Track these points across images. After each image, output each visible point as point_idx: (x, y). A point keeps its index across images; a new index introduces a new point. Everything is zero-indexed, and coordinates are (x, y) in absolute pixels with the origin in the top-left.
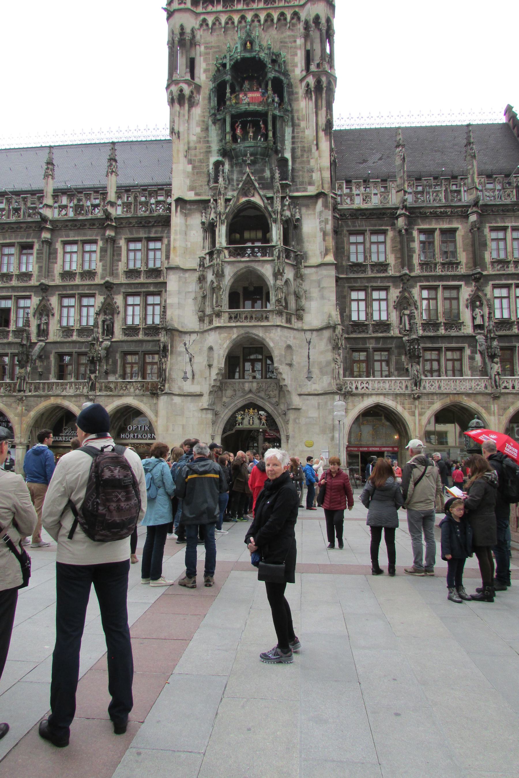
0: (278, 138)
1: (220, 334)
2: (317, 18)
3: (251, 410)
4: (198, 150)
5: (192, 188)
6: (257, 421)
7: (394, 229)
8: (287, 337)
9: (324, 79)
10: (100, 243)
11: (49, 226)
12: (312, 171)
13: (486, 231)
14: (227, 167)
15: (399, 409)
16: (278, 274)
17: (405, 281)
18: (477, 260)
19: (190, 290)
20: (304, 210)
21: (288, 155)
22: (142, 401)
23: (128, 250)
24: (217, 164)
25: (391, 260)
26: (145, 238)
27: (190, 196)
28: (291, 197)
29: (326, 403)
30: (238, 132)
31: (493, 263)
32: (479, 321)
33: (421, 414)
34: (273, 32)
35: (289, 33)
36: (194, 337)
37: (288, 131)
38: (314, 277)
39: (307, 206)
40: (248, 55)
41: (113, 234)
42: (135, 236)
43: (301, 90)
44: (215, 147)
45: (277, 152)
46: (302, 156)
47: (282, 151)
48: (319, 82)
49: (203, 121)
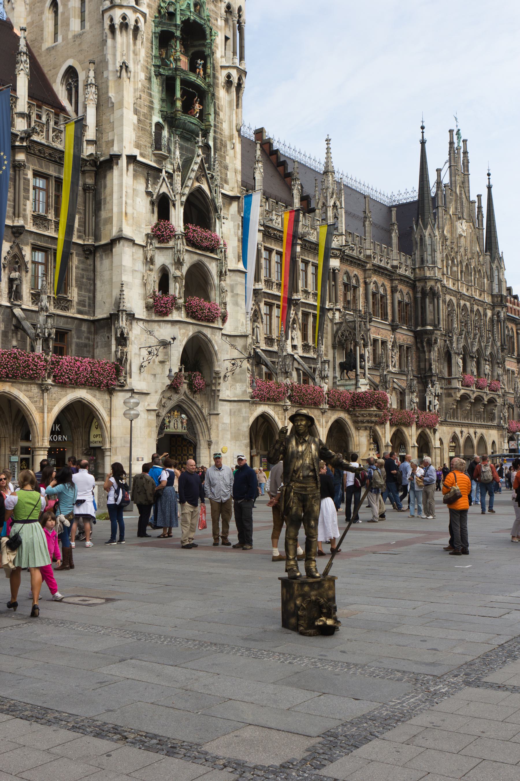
1: (180, 329)
3: (176, 413)
4: (142, 101)
5: (138, 146)
6: (180, 425)
14: (165, 133)
19: (136, 269)
21: (211, 143)
22: (95, 396)
26: (55, 177)
29: (240, 411)
32: (295, 343)
36: (141, 323)
40: (198, 20)
42: (44, 170)
44: (157, 105)
46: (221, 148)
49: (147, 68)
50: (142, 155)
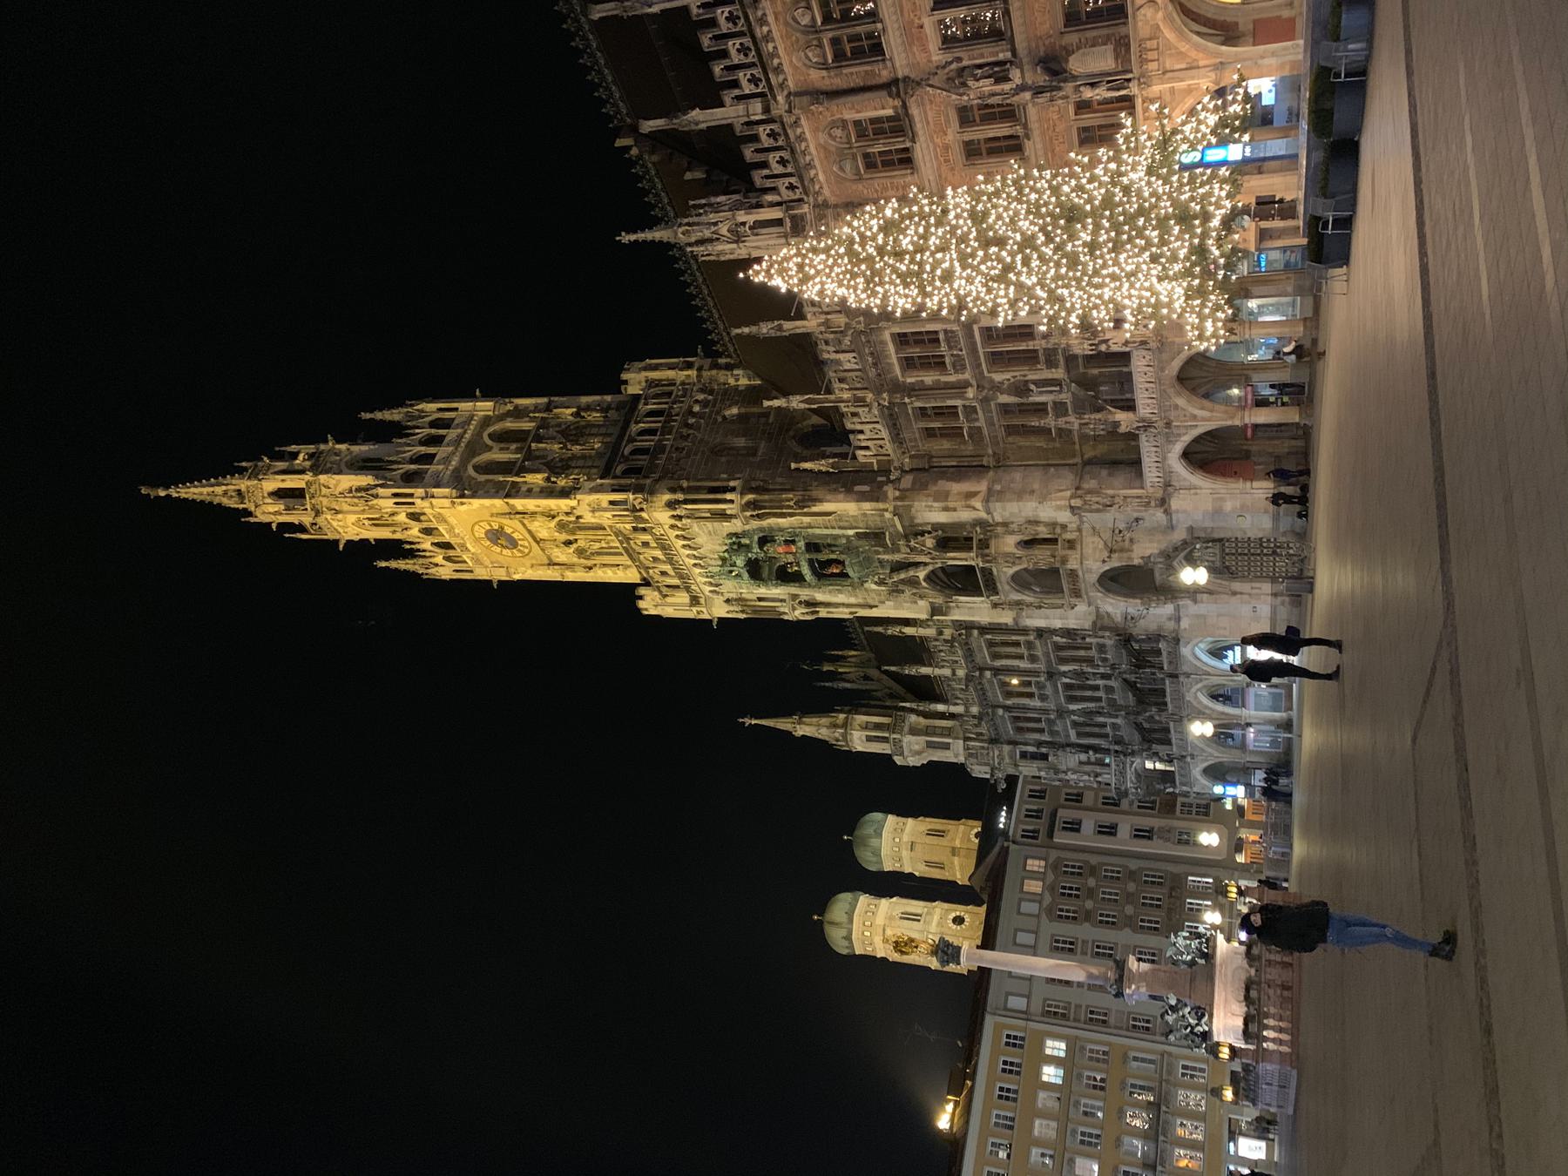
8: (1095, 549)
15: (1187, 439)
16: (1012, 559)
21: (851, 532)
33: (1194, 417)
34: (699, 540)
37: (818, 531)
39: (912, 518)
40: (746, 576)
41: (975, 632)
47: (848, 537)
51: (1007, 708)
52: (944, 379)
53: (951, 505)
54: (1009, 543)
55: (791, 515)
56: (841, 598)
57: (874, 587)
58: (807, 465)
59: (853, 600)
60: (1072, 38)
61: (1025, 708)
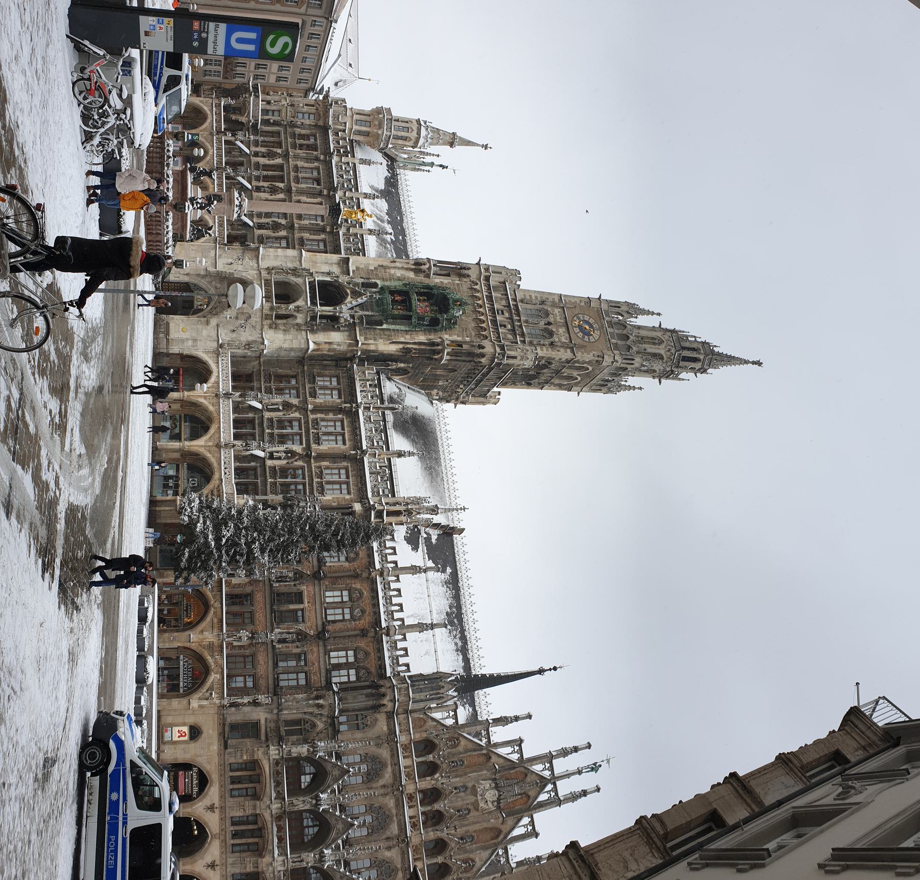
0: (395, 319)
2: (483, 347)
5: (358, 268)
7: (342, 402)
9: (440, 347)
10: (322, 224)
11: (331, 193)
12: (375, 340)
13: (345, 464)
16: (298, 309)
17: (303, 409)
18: (321, 457)
20: (347, 333)
21: (385, 326)
23: (318, 241)
24: (375, 285)
25: (320, 400)
27: (352, 267)
28: (354, 322)
30: (398, 298)
31: (320, 467)
34: (473, 325)
35: (473, 334)
37: (403, 328)
38: (299, 337)
39: (349, 336)
40: (451, 302)
43: (432, 337)
44: (387, 283)
45: (386, 319)
47: (387, 323)
48: (438, 345)
50: (353, 271)
51: (317, 159)
52: (323, 416)
53: (327, 346)
54: (300, 318)
55: (415, 343)
56: (399, 273)
57: (378, 282)
58: (402, 365)
59: (392, 271)
60: (248, 589)
61: (307, 160)
